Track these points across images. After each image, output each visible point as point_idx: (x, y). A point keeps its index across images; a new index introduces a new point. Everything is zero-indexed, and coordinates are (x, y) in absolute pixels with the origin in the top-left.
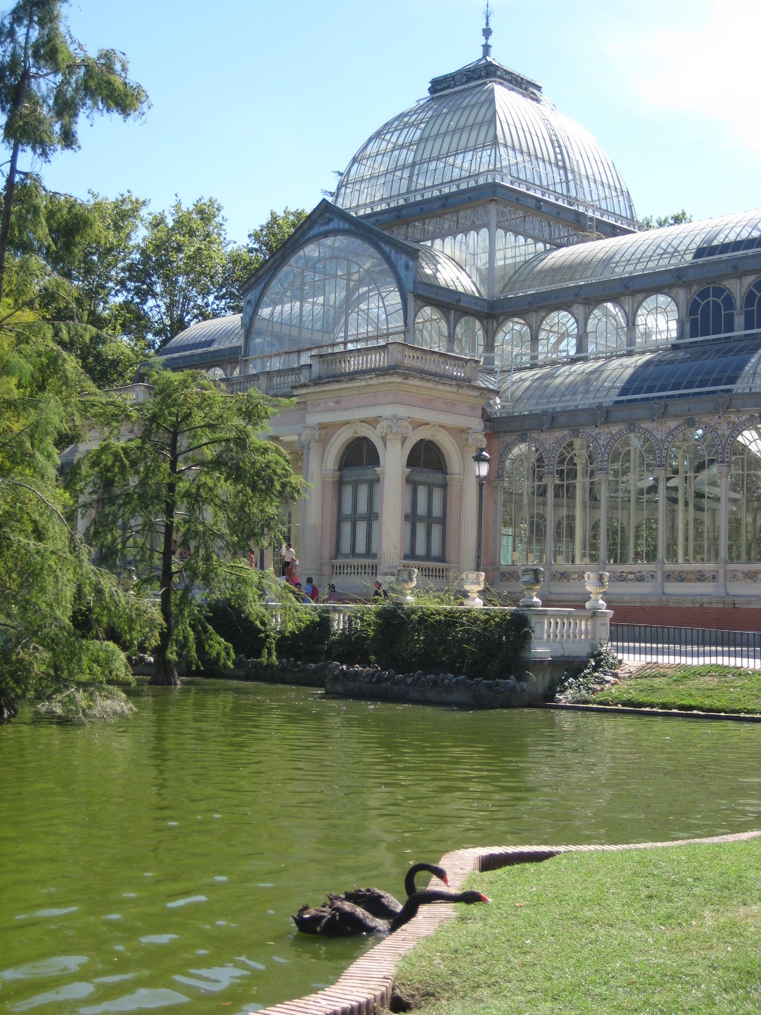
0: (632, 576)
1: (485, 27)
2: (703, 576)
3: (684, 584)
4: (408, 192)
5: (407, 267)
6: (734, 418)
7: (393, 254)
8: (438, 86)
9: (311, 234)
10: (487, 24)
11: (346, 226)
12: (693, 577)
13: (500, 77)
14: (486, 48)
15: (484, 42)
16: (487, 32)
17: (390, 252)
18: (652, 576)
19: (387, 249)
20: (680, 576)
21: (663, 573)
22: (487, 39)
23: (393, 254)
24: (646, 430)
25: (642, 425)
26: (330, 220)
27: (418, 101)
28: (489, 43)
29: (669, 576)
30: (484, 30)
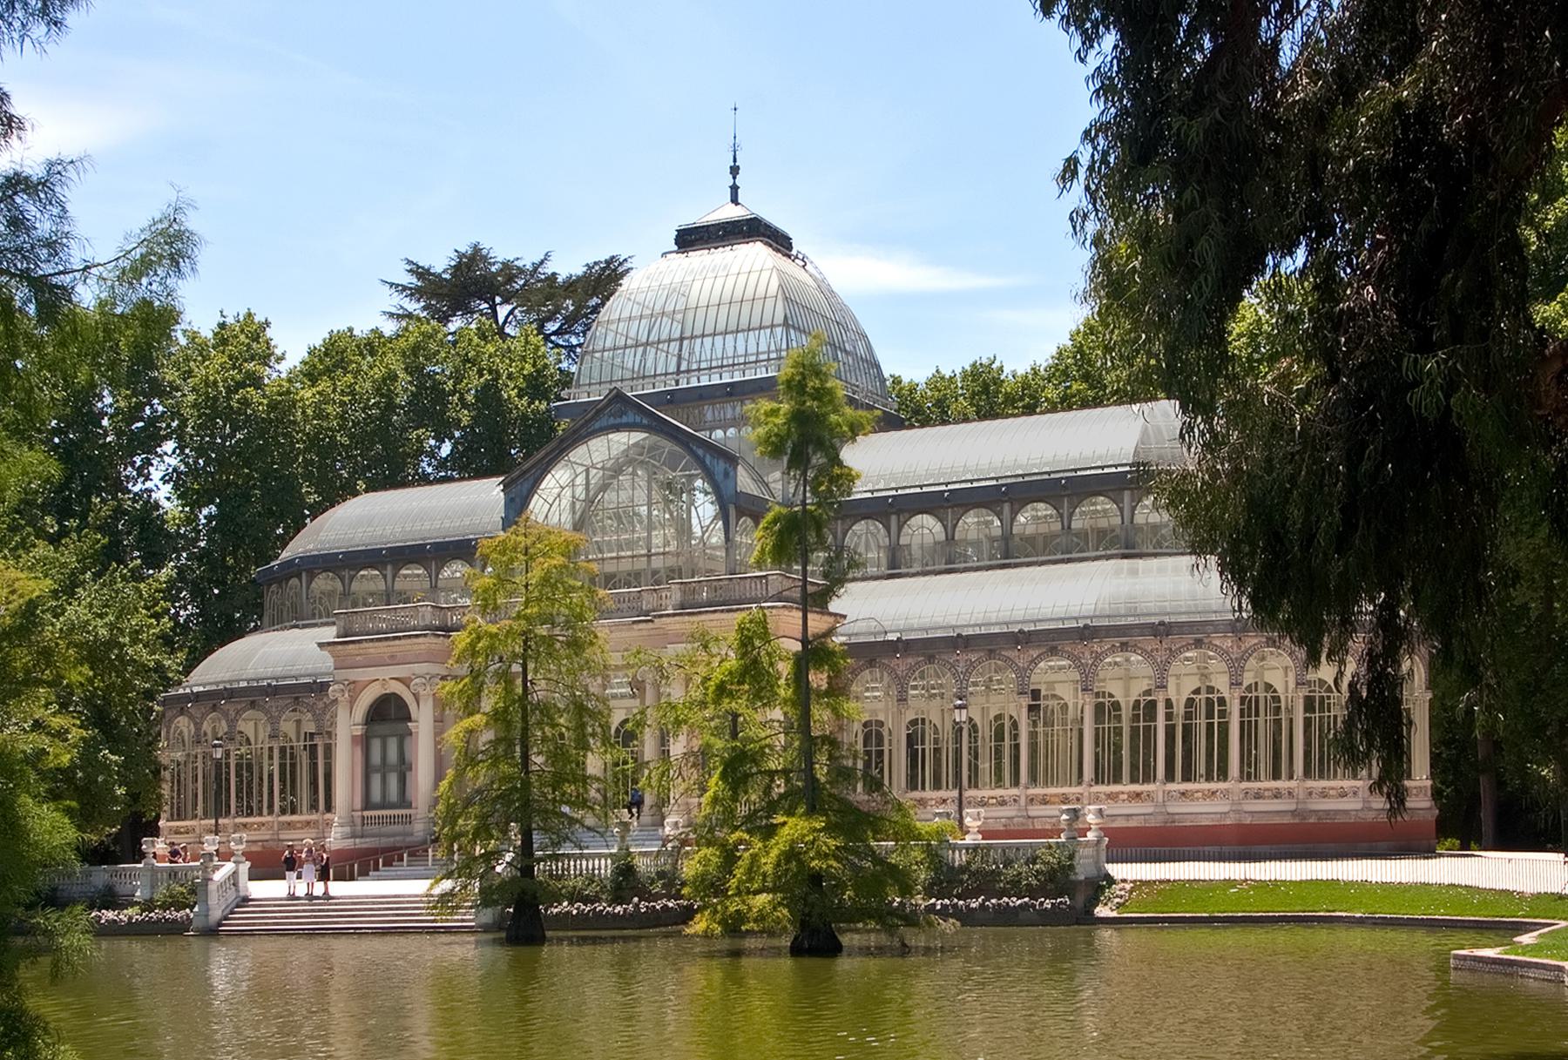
0: (994, 801)
2: (1067, 799)
3: (1048, 807)
4: (678, 372)
8: (690, 239)
10: (735, 161)
12: (1057, 800)
13: (764, 236)
14: (734, 189)
15: (731, 184)
16: (735, 171)
18: (1015, 800)
20: (1044, 800)
21: (1027, 797)
22: (734, 178)
29: (1032, 800)
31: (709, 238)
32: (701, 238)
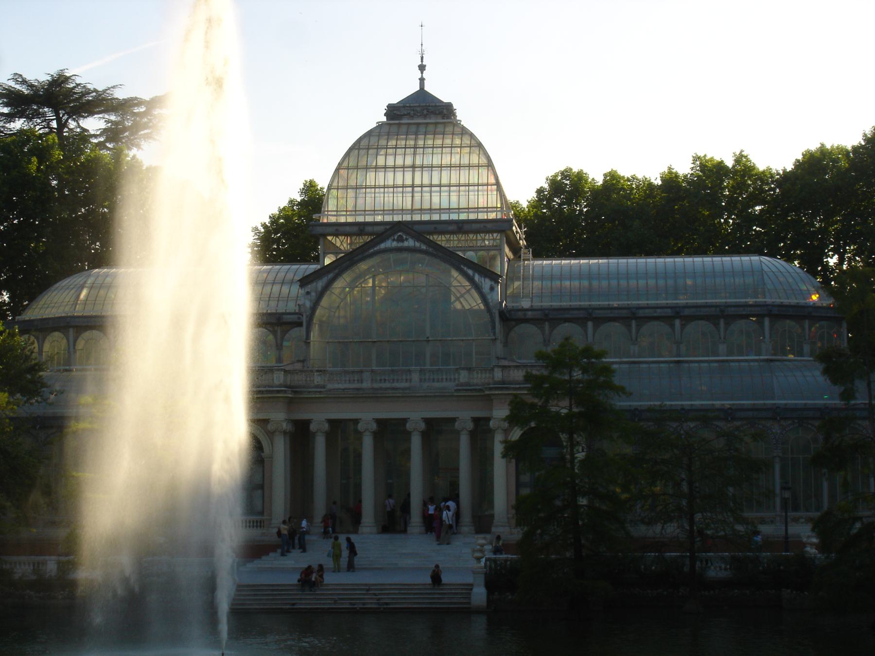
1: (421, 63)
5: (492, 289)
6: (782, 422)
7: (477, 277)
9: (383, 246)
11: (424, 247)
14: (422, 80)
15: (420, 77)
16: (422, 68)
17: (474, 275)
19: (470, 272)
22: (422, 73)
23: (477, 277)
24: (717, 426)
25: (714, 423)
26: (407, 239)
27: (377, 123)
28: (424, 76)
30: (419, 66)
31: (414, 114)
32: (409, 114)
